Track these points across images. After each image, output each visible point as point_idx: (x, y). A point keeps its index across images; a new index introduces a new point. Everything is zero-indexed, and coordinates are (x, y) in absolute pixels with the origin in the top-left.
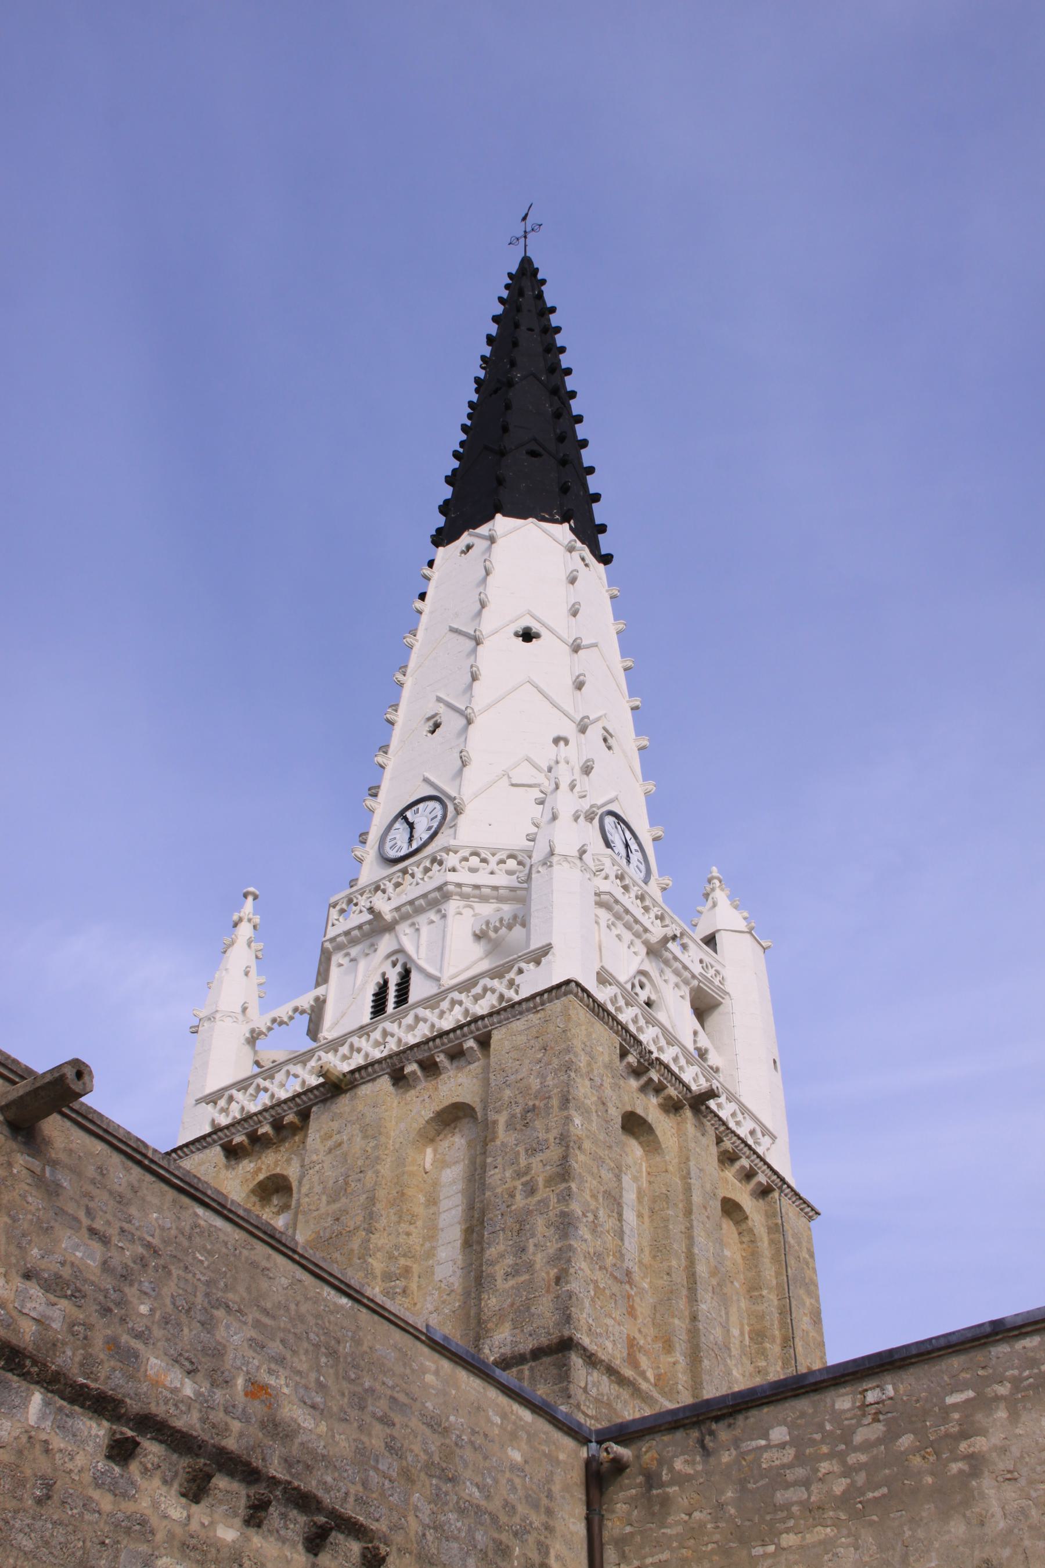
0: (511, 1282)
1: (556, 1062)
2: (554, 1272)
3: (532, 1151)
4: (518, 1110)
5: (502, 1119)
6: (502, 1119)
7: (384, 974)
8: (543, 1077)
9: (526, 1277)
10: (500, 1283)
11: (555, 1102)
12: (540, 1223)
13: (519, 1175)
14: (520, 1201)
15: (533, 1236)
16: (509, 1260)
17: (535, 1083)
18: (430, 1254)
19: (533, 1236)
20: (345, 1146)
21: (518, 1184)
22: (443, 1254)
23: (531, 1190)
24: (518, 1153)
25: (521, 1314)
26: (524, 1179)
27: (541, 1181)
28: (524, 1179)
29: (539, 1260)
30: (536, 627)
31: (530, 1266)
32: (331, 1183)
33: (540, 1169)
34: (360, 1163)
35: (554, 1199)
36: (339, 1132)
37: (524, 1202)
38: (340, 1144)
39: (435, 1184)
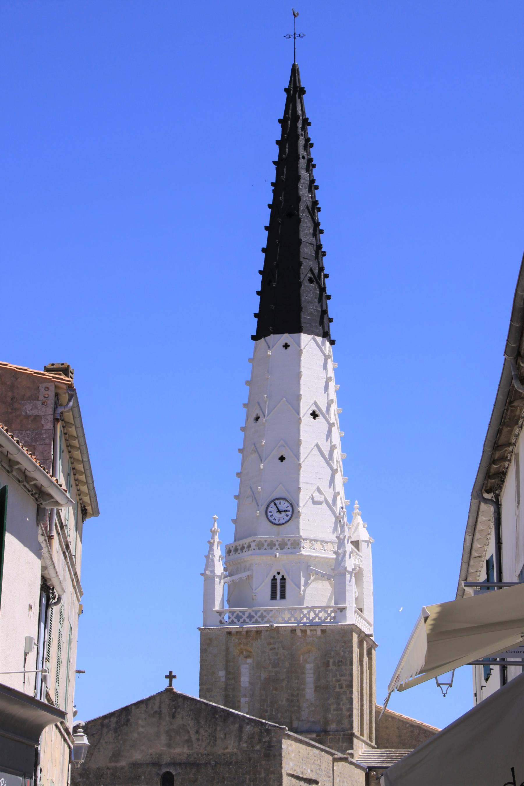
0: (335, 712)
1: (348, 649)
2: (348, 713)
3: (342, 675)
4: (337, 660)
5: (331, 661)
6: (331, 661)
7: (274, 576)
8: (345, 653)
9: (339, 712)
10: (332, 711)
11: (348, 662)
12: (344, 697)
13: (337, 681)
14: (338, 689)
15: (342, 701)
16: (335, 706)
17: (342, 653)
18: (304, 689)
19: (342, 701)
20: (276, 650)
21: (337, 684)
22: (308, 691)
23: (341, 687)
24: (336, 675)
25: (339, 722)
26: (339, 683)
27: (344, 686)
28: (339, 683)
29: (344, 708)
30: (317, 412)
31: (341, 709)
32: (272, 661)
33: (345, 684)
34: (283, 658)
35: (348, 693)
36: (274, 644)
37: (338, 690)
38: (275, 648)
39: (304, 667)
